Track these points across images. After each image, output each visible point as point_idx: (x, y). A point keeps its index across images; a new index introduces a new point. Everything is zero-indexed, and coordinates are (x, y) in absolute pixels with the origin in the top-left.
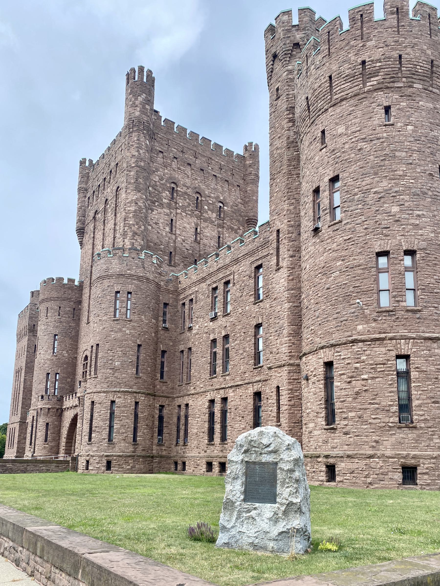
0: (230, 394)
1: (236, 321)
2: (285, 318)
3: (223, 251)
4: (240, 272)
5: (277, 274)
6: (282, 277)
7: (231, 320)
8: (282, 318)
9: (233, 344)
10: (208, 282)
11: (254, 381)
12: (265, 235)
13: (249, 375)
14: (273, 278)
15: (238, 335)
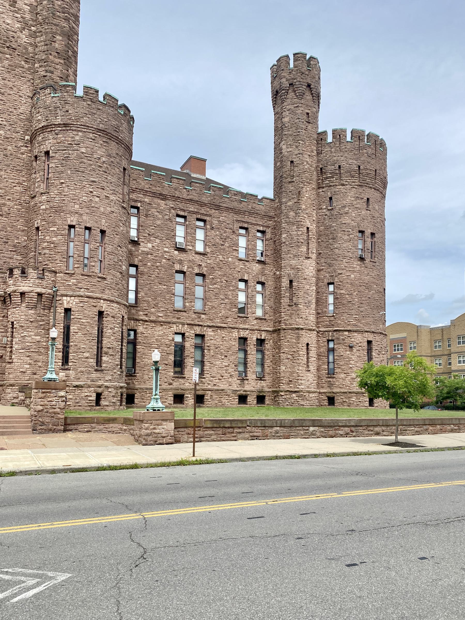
0: (209, 333)
1: (216, 265)
2: (313, 296)
3: (198, 185)
4: (220, 219)
5: (306, 261)
6: (311, 265)
7: (209, 262)
8: (310, 295)
9: (210, 286)
10: (171, 204)
11: (241, 328)
12: (254, 205)
13: (232, 321)
14: (303, 262)
15: (219, 280)
